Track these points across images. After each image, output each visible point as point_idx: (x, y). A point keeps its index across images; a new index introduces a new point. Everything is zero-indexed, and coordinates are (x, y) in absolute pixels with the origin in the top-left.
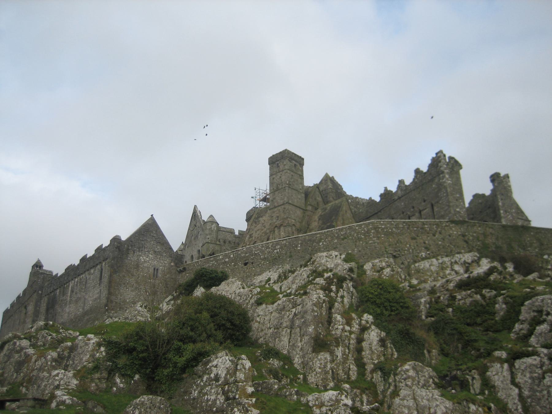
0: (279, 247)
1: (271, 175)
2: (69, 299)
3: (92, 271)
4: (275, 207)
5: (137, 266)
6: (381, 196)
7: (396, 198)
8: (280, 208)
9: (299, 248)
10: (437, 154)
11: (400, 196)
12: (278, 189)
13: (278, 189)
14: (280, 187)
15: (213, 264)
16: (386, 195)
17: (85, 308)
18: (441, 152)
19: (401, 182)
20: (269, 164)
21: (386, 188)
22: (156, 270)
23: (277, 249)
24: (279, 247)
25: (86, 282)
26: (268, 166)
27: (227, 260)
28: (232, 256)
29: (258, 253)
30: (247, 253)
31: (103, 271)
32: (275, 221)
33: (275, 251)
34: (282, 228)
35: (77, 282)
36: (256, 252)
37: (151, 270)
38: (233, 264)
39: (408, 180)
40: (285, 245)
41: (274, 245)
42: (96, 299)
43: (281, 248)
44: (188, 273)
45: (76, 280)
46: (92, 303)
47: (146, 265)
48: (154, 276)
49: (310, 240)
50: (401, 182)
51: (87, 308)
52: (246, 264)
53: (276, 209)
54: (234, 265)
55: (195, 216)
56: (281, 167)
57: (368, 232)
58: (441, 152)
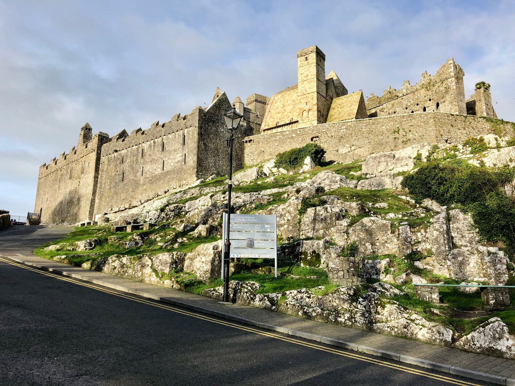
0: (344, 127)
8: (308, 95)
9: (364, 130)
11: (405, 94)
15: (280, 138)
17: (165, 168)
24: (344, 127)
27: (294, 135)
28: (299, 132)
30: (313, 131)
31: (186, 138)
33: (341, 131)
36: (323, 131)
38: (300, 139)
40: (351, 127)
41: (340, 126)
42: (179, 161)
46: (174, 165)
48: (228, 146)
53: (304, 96)
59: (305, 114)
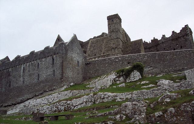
1: (109, 24)
2: (22, 73)
3: (43, 60)
4: (112, 39)
5: (72, 60)
6: (152, 40)
7: (161, 42)
10: (185, 26)
12: (113, 31)
13: (113, 31)
14: (115, 30)
15: (108, 62)
16: (155, 41)
17: (40, 79)
18: (187, 25)
19: (164, 36)
20: (108, 19)
21: (154, 38)
22: (78, 62)
23: (145, 58)
25: (38, 66)
26: (107, 21)
27: (117, 60)
29: (136, 58)
30: (128, 58)
32: (112, 45)
34: (116, 49)
35: (29, 65)
37: (77, 62)
39: (168, 35)
42: (50, 75)
43: (148, 57)
44: (92, 65)
45: (28, 64)
47: (75, 59)
49: (162, 55)
50: (164, 36)
51: (42, 78)
52: (128, 63)
53: (112, 40)
54: (122, 63)
55: (59, 39)
56: (115, 21)
57: (190, 54)
58: (187, 25)
59: (113, 50)
